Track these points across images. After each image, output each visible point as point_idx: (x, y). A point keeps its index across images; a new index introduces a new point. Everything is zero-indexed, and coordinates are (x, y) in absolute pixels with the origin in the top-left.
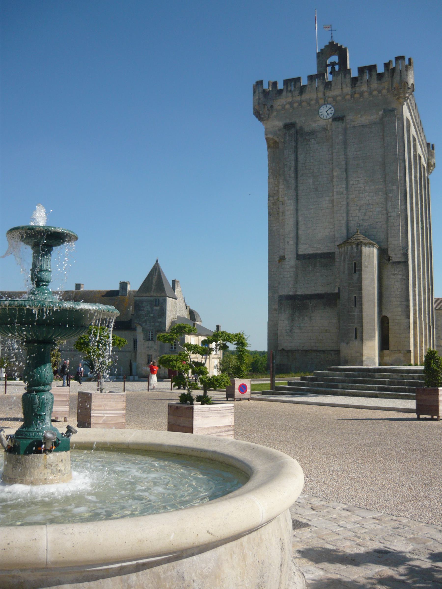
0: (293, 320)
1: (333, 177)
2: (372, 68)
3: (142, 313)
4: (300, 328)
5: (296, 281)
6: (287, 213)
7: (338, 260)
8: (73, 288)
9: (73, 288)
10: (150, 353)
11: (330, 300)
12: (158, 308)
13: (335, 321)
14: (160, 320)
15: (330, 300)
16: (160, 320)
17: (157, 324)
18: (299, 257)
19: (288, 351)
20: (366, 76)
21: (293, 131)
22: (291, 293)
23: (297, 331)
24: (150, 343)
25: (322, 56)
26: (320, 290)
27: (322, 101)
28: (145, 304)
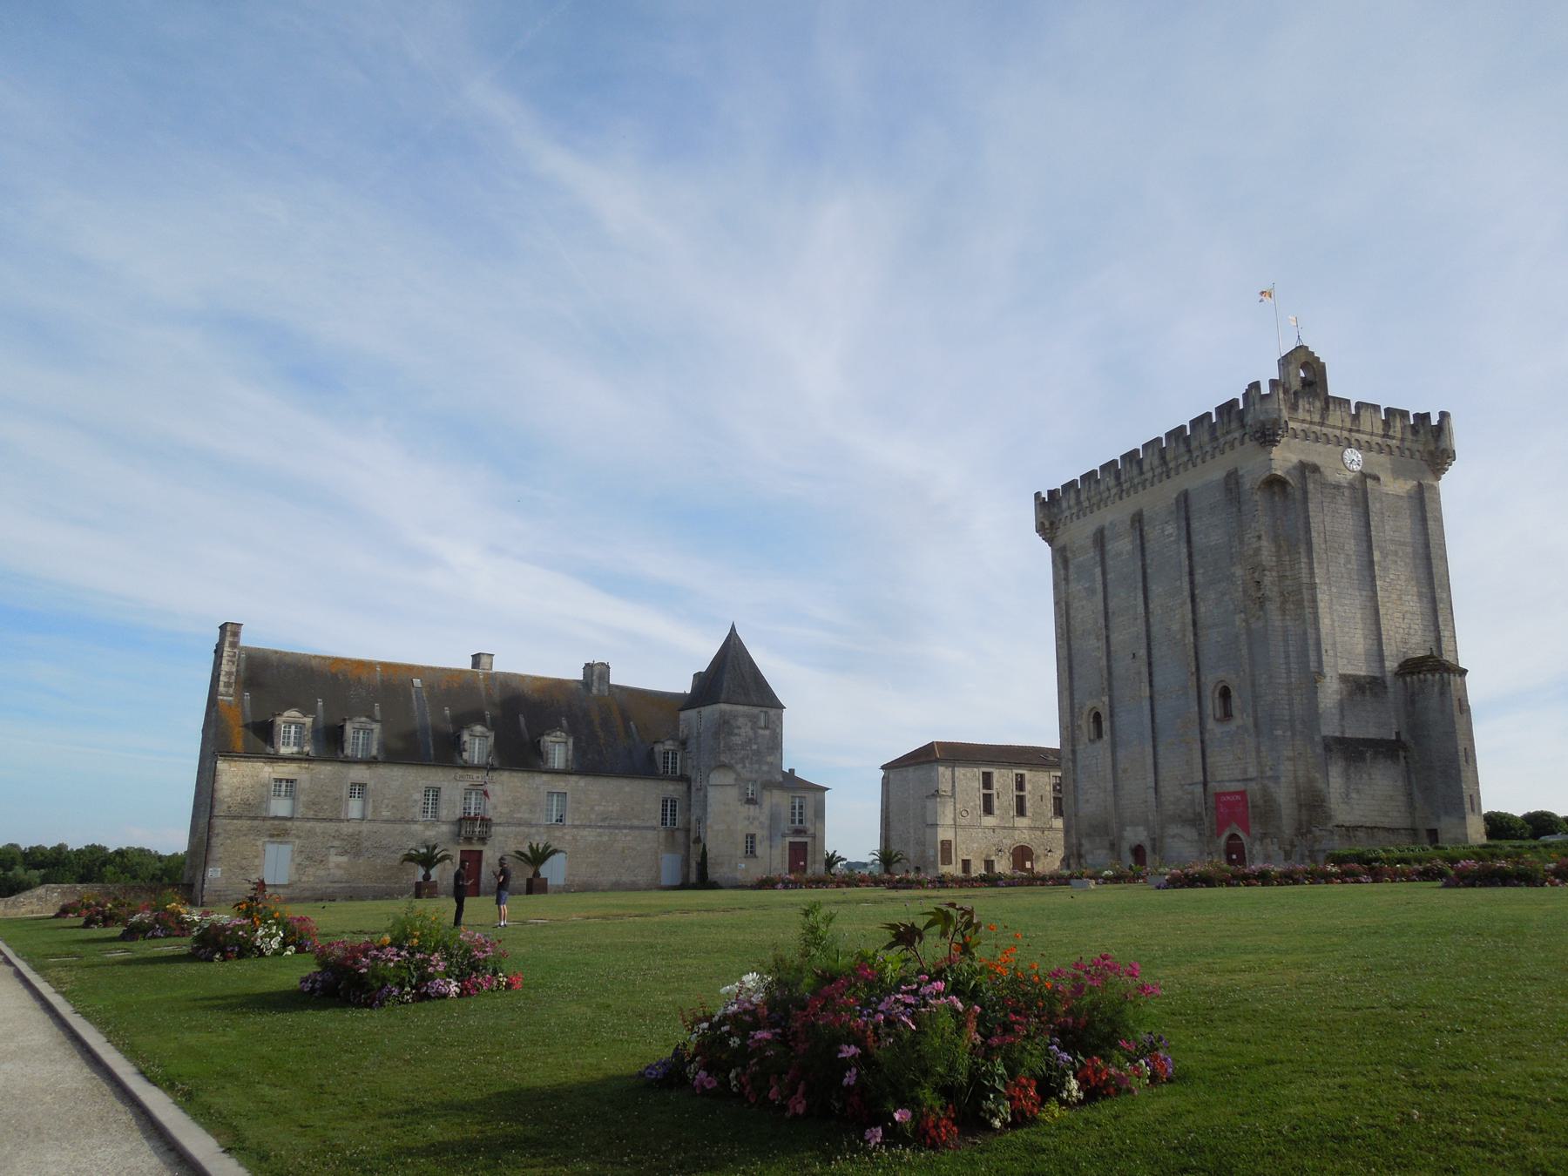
0: (1348, 778)
1: (1371, 563)
2: (1404, 414)
3: (737, 740)
4: (1358, 792)
5: (1343, 717)
6: (1321, 605)
7: (1391, 690)
8: (467, 665)
9: (467, 665)
10: (752, 831)
11: (1388, 749)
12: (767, 732)
13: (1400, 783)
14: (770, 759)
15: (1388, 749)
16: (770, 759)
17: (765, 768)
18: (1344, 678)
19: (1348, 828)
20: (1398, 424)
21: (1317, 476)
22: (1337, 734)
23: (1354, 795)
24: (753, 810)
25: (1285, 362)
26: (1372, 733)
27: (1345, 443)
28: (741, 721)
